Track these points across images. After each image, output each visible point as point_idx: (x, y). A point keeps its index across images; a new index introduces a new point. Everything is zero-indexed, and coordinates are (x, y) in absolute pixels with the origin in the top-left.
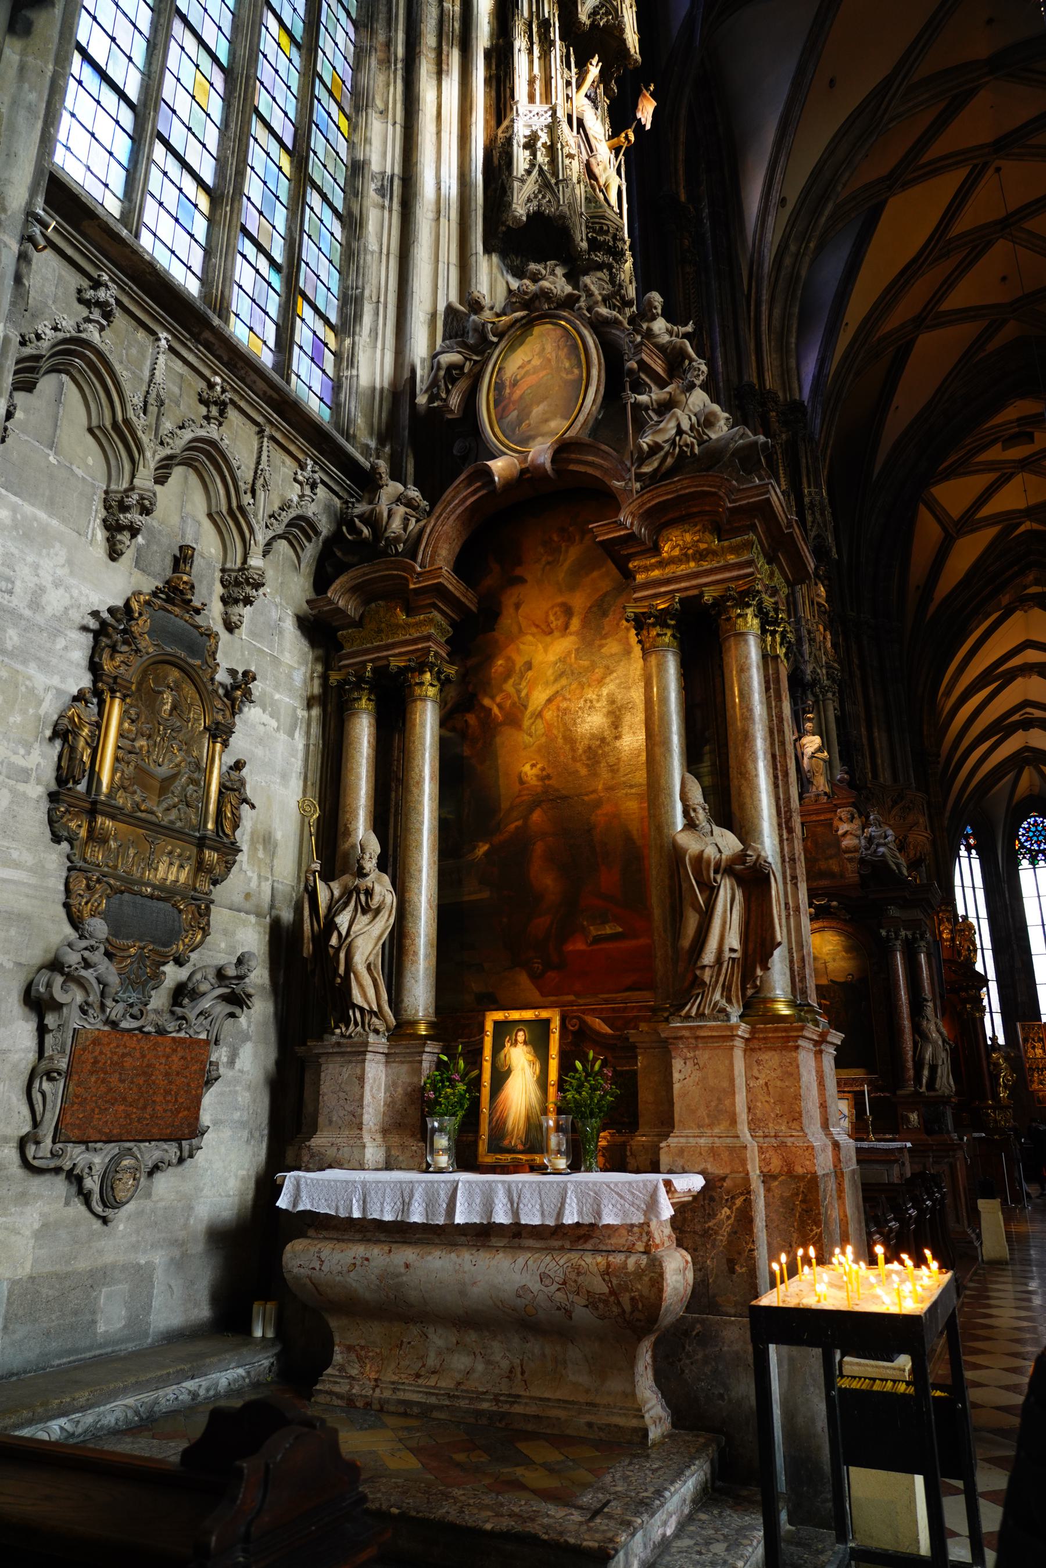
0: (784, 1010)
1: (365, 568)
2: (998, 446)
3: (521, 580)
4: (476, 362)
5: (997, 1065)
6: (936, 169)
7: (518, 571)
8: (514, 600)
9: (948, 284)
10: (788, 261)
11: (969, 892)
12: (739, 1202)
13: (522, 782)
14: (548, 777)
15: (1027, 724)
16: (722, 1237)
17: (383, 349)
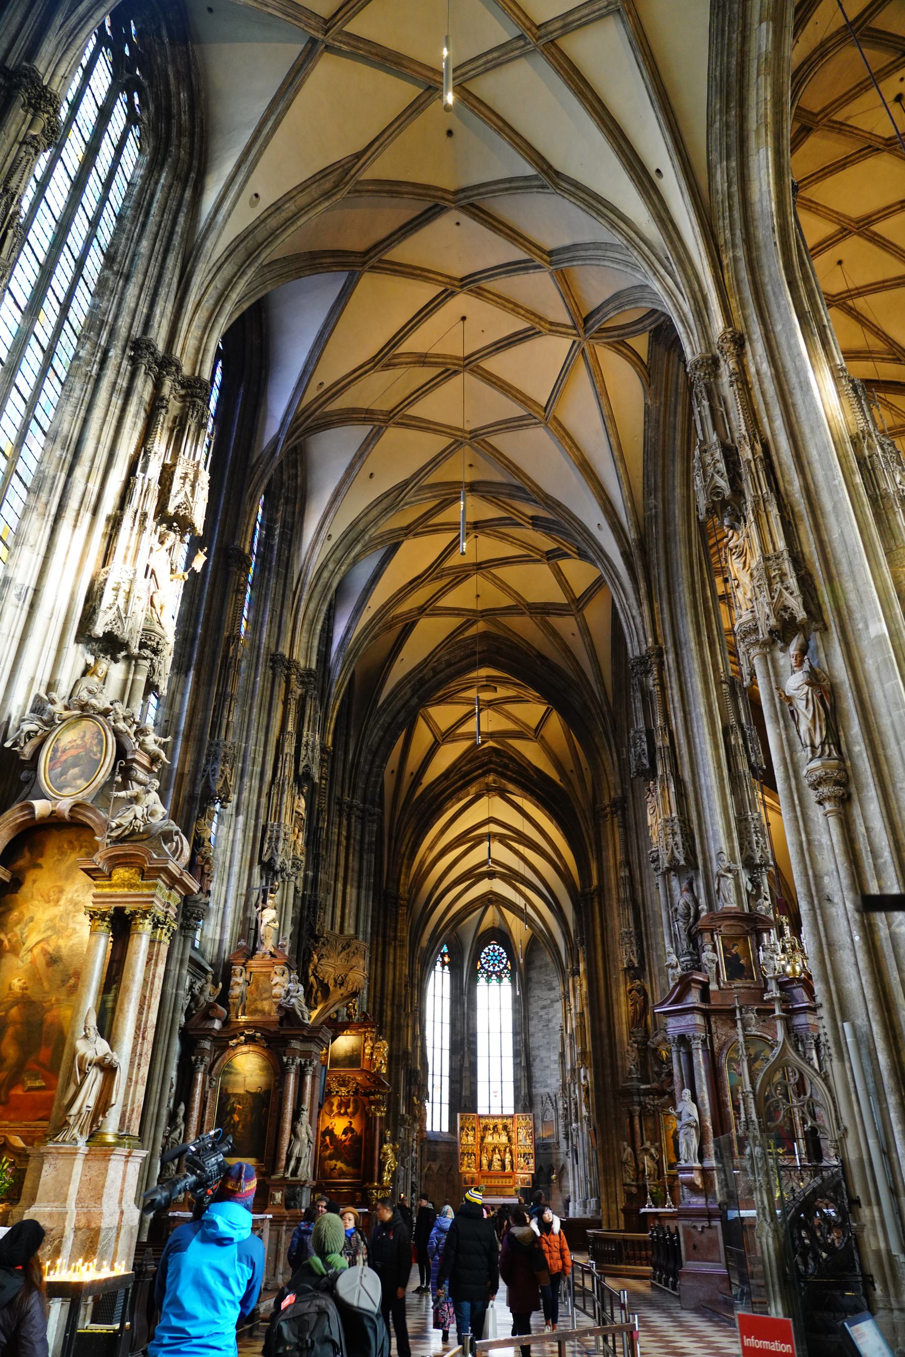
0: (110, 1139)
2: (474, 690)
3: (39, 866)
5: (385, 1154)
6: (437, 529)
7: (40, 861)
8: (33, 877)
9: (443, 592)
10: (326, 574)
11: (438, 1000)
12: (56, 1242)
13: (10, 989)
14: (26, 989)
15: (491, 875)
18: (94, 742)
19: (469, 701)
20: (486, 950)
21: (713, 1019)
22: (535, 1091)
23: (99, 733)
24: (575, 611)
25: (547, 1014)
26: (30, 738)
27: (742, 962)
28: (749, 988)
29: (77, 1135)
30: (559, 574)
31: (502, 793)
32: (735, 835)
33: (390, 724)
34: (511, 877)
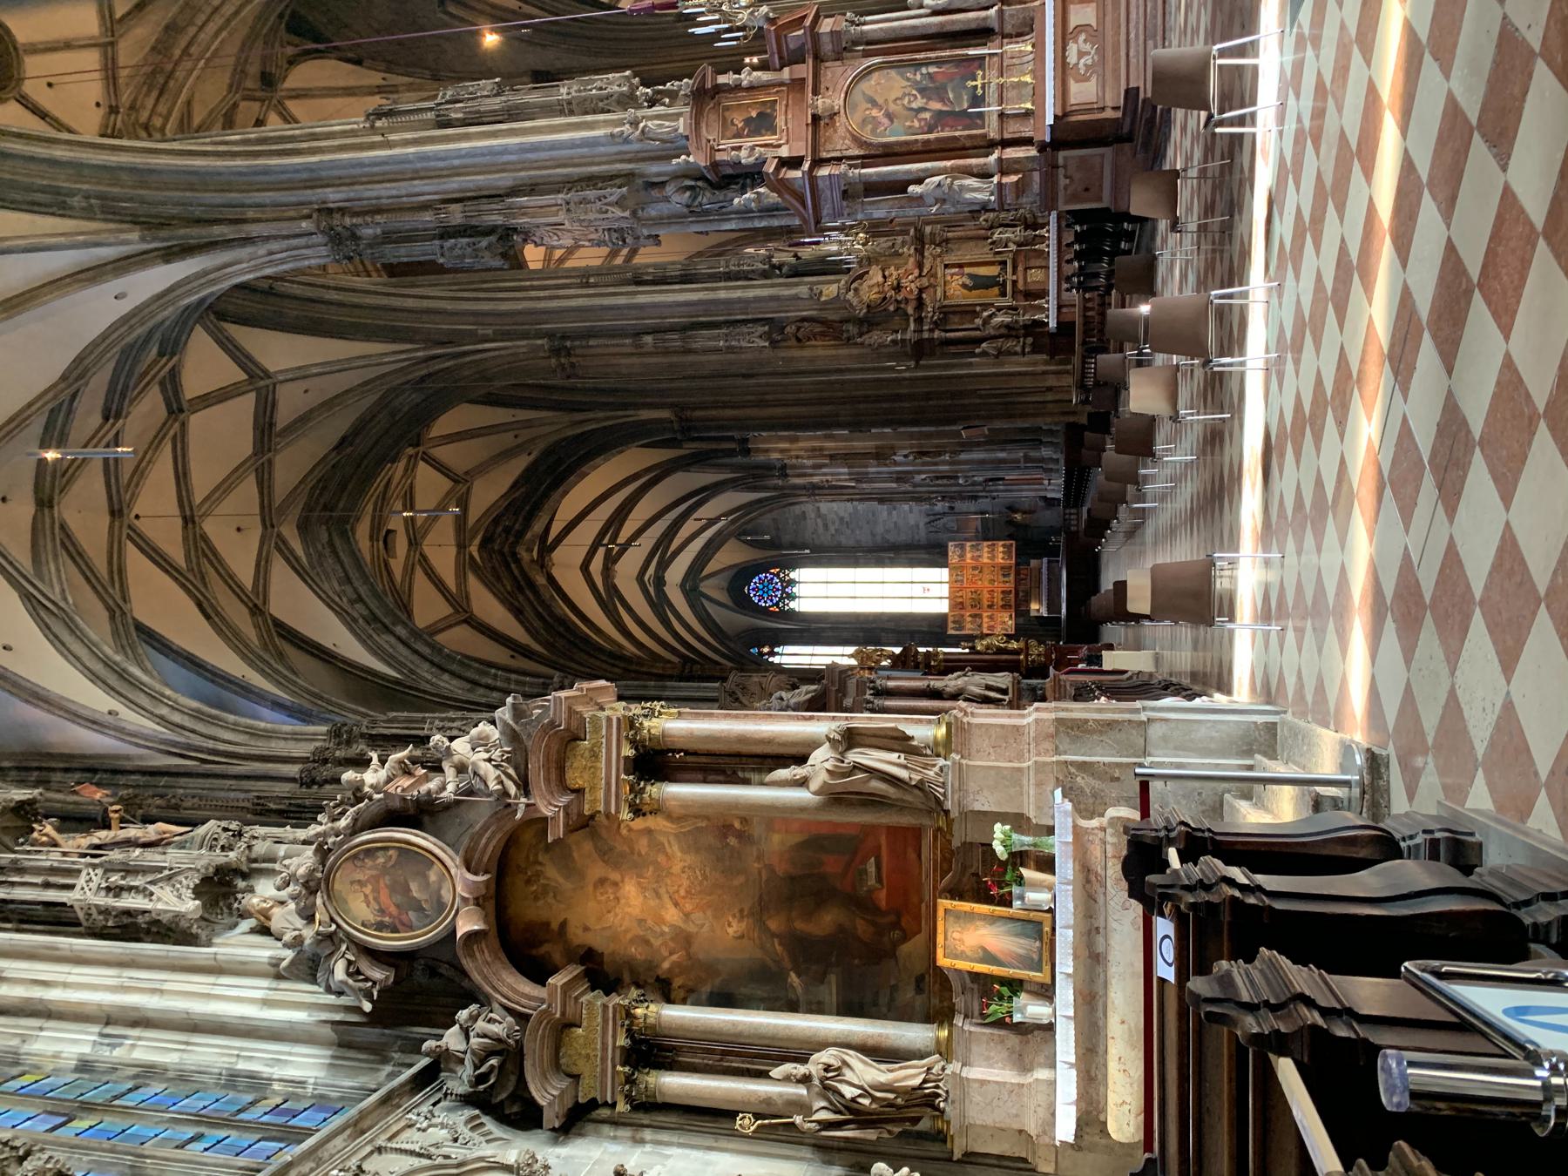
1: (528, 1064)
2: (392, 562)
3: (563, 925)
4: (347, 949)
5: (988, 647)
6: (118, 571)
7: (555, 926)
8: (579, 932)
9: (230, 580)
10: (177, 718)
12: (1073, 770)
13: (742, 937)
14: (741, 911)
15: (660, 581)
16: (1096, 784)
17: (290, 1054)
18: (369, 862)
19: (409, 571)
20: (756, 600)
21: (824, 155)
22: (924, 541)
23: (355, 857)
24: (268, 382)
25: (833, 523)
26: (358, 972)
27: (754, 114)
28: (787, 106)
29: (936, 769)
30: (207, 400)
31: (547, 549)
32: (589, 118)
33: (432, 663)
34: (663, 553)
